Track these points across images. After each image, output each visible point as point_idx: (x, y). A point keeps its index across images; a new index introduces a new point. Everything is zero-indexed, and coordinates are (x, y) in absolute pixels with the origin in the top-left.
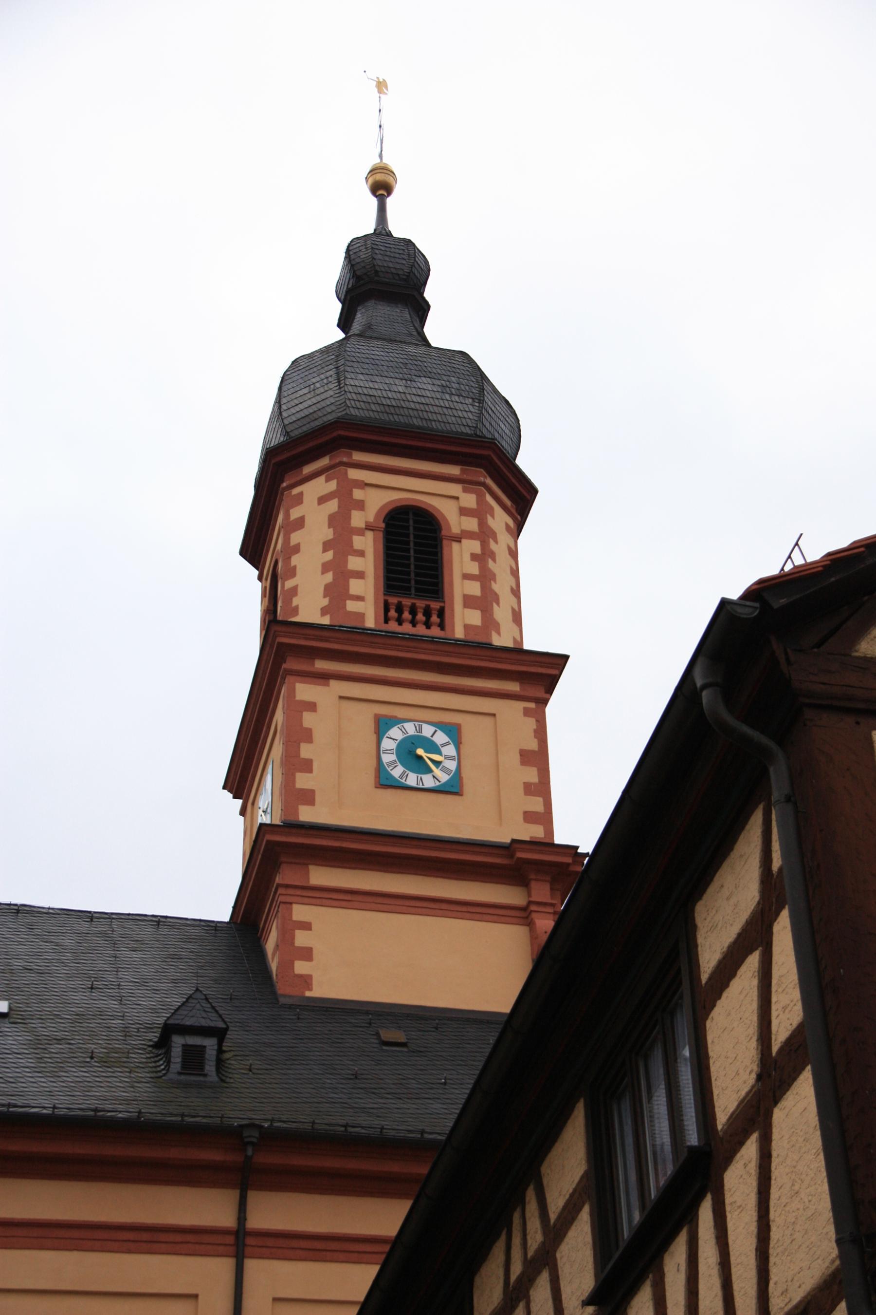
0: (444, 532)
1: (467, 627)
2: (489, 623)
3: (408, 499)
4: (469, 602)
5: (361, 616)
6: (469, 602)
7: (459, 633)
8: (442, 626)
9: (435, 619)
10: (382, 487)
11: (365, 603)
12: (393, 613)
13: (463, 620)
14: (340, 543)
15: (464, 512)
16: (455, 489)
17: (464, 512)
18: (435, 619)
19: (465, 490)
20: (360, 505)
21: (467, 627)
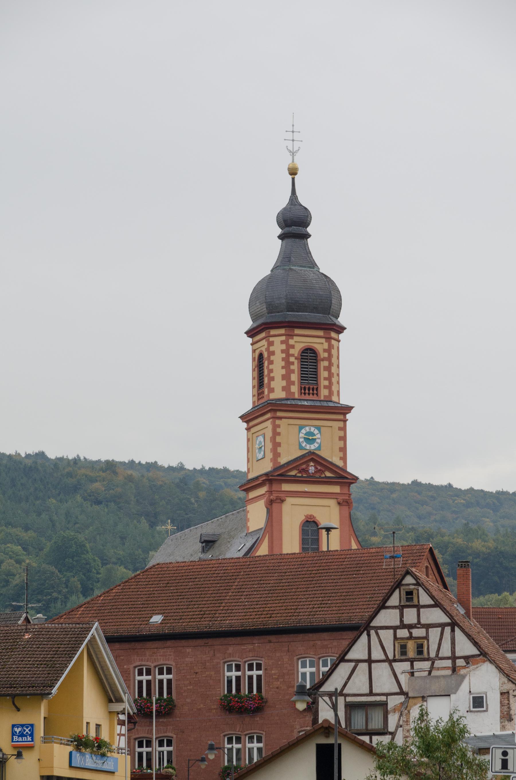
0: (319, 358)
1: (325, 396)
2: (331, 393)
3: (308, 346)
4: (325, 387)
5: (294, 393)
6: (325, 387)
7: (322, 398)
8: (317, 394)
9: (315, 392)
10: (301, 341)
11: (295, 389)
12: (303, 391)
13: (324, 393)
14: (288, 364)
15: (325, 351)
16: (323, 340)
17: (325, 351)
18: (315, 392)
19: (326, 342)
20: (293, 347)
21: (325, 396)
